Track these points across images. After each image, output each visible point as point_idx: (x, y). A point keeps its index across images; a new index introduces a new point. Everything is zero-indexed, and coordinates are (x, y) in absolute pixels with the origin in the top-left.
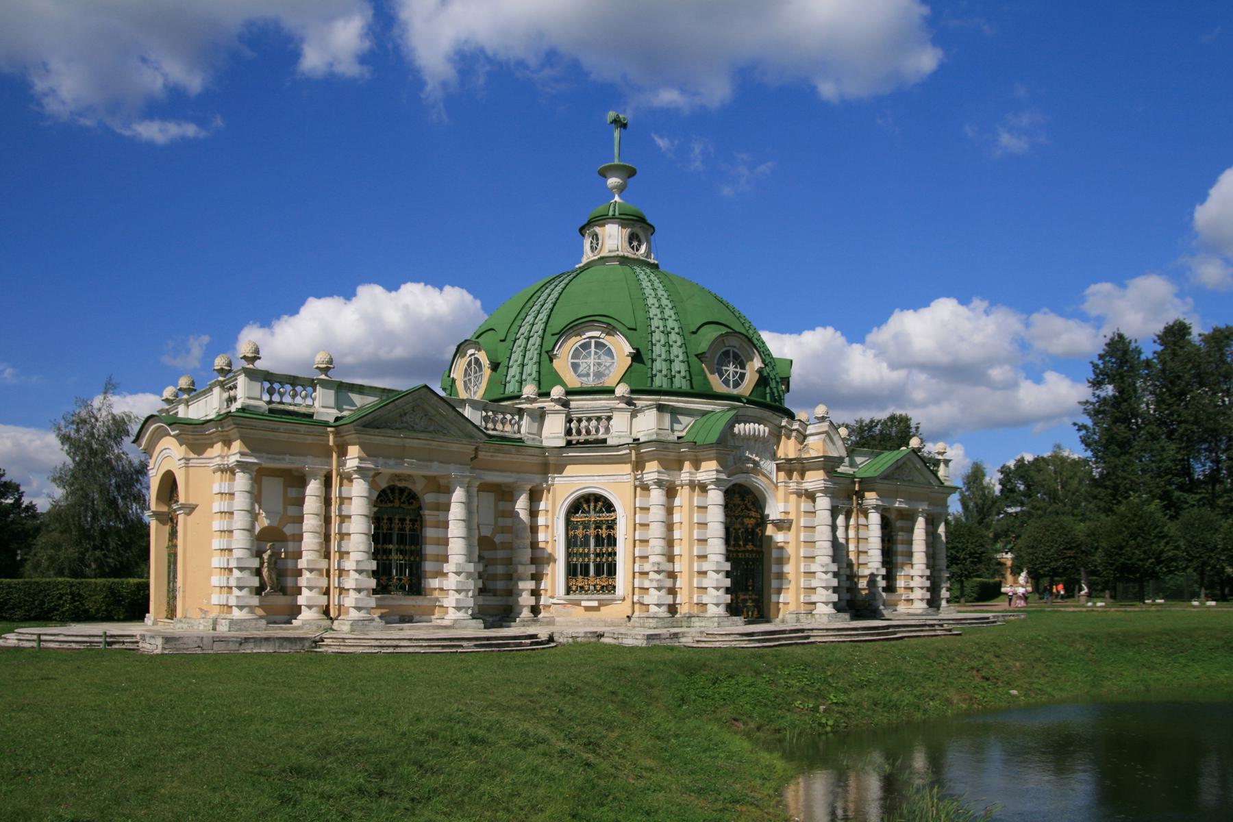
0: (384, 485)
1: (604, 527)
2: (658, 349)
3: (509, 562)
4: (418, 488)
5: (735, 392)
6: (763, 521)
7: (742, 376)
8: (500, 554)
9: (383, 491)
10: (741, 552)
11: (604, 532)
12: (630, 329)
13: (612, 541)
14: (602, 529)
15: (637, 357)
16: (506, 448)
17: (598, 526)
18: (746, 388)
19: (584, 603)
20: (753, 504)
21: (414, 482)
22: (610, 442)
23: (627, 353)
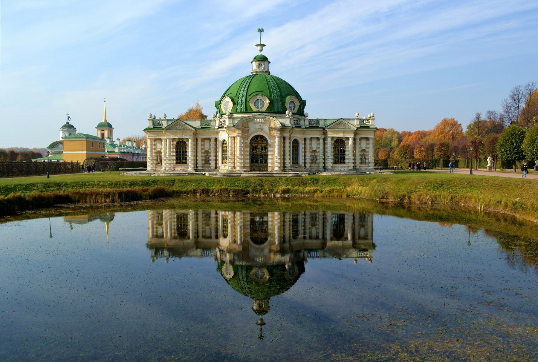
0: (177, 141)
2: (240, 101)
4: (185, 141)
5: (261, 110)
6: (267, 145)
7: (263, 105)
9: (178, 142)
15: (234, 104)
16: (205, 130)
18: (264, 109)
20: (265, 140)
21: (184, 139)
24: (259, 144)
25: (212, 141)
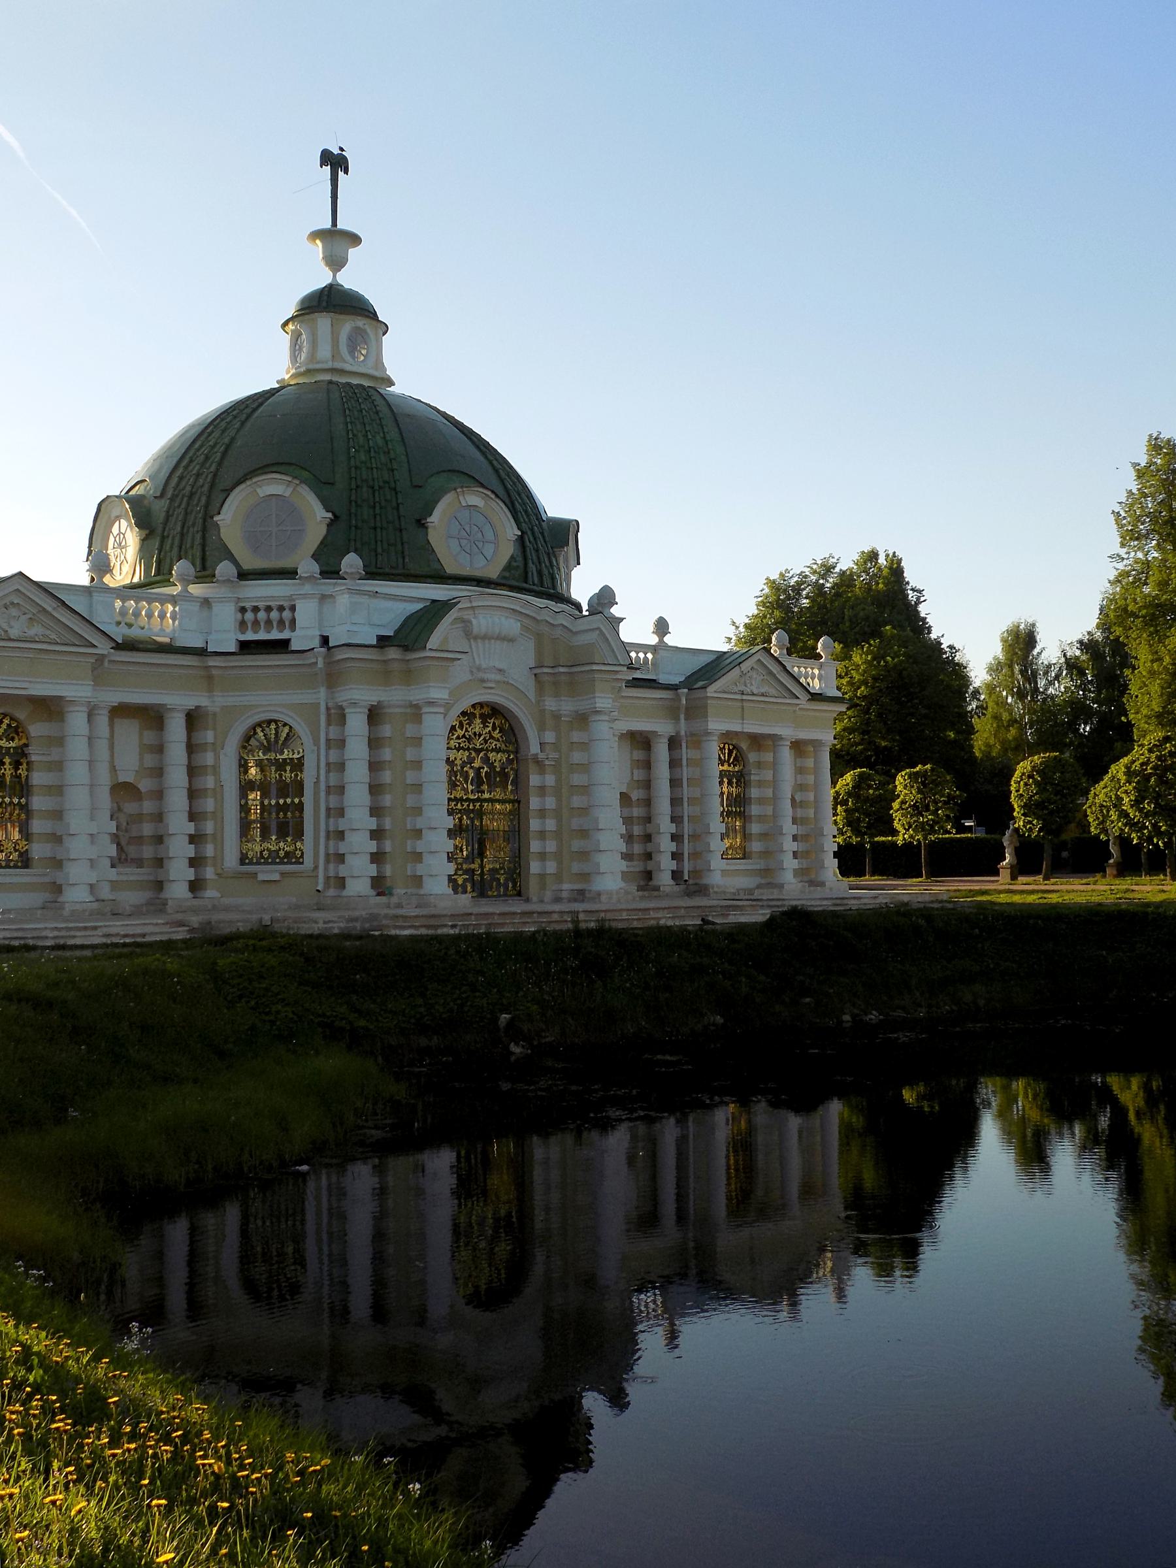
1: (288, 768)
3: (159, 817)
8: (148, 806)
10: (486, 800)
11: (288, 775)
12: (325, 483)
13: (299, 787)
14: (285, 772)
17: (281, 766)
19: (261, 877)
22: (294, 646)
23: (319, 519)
24: (478, 751)
25: (176, 729)
